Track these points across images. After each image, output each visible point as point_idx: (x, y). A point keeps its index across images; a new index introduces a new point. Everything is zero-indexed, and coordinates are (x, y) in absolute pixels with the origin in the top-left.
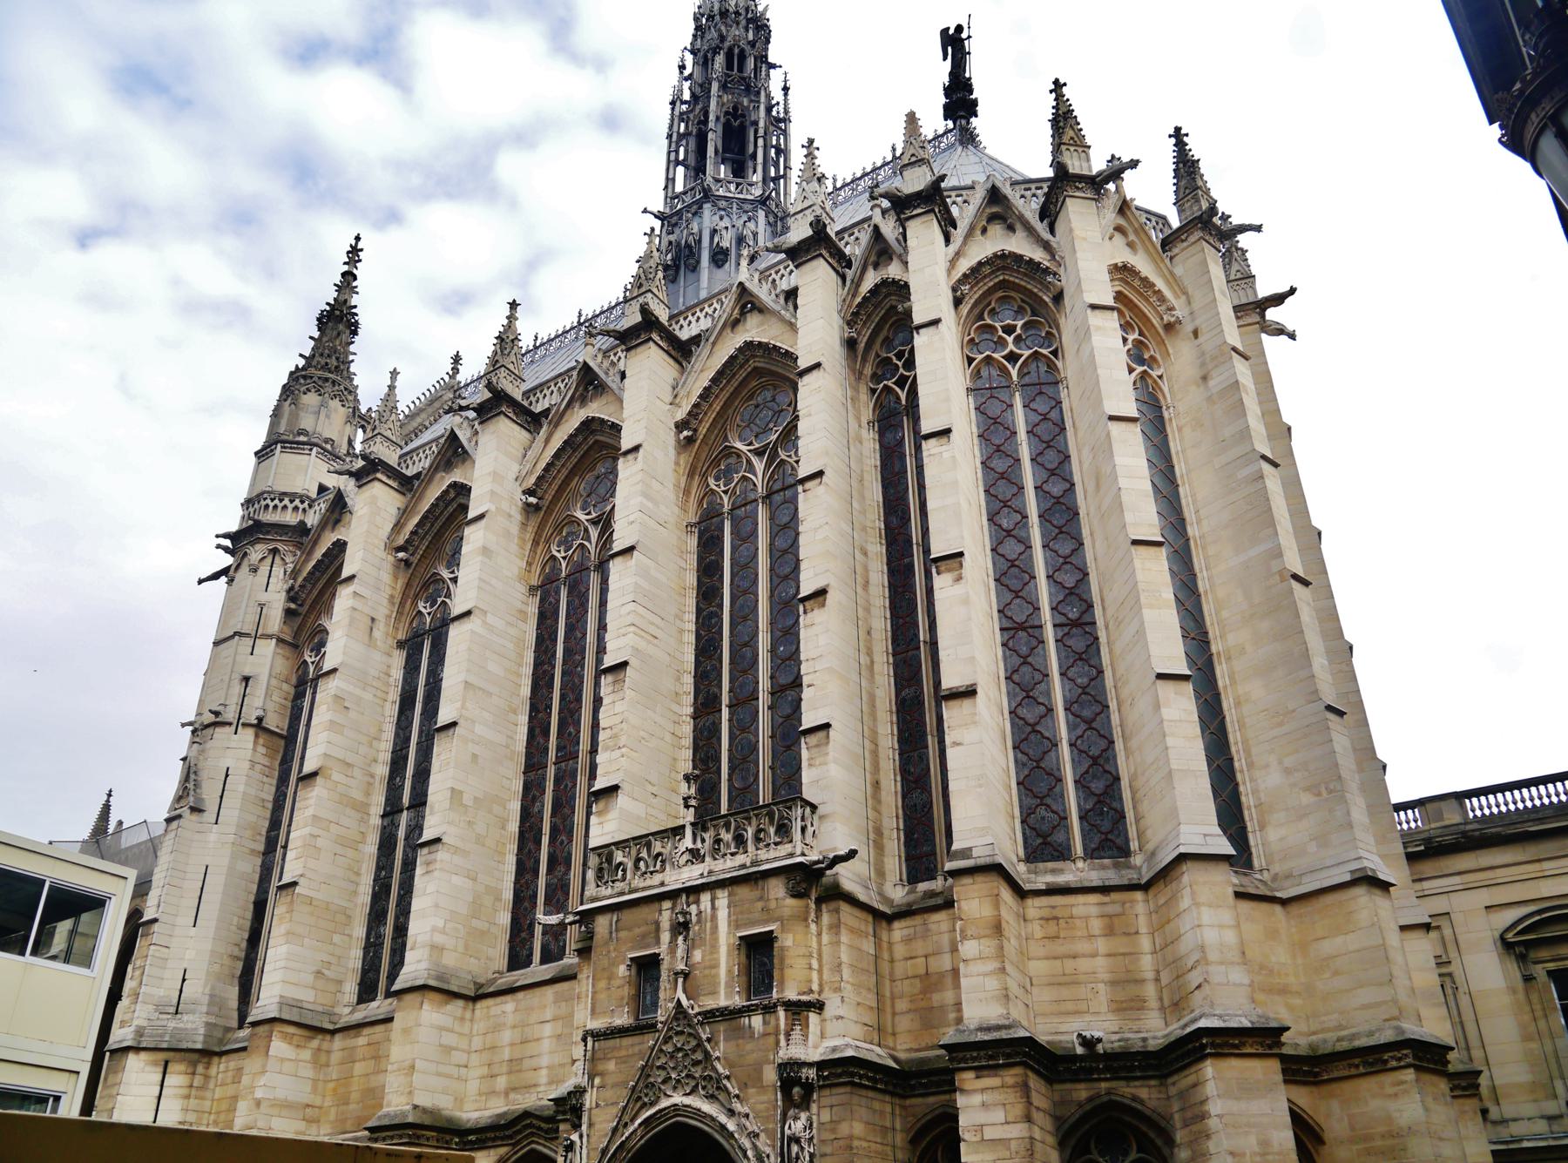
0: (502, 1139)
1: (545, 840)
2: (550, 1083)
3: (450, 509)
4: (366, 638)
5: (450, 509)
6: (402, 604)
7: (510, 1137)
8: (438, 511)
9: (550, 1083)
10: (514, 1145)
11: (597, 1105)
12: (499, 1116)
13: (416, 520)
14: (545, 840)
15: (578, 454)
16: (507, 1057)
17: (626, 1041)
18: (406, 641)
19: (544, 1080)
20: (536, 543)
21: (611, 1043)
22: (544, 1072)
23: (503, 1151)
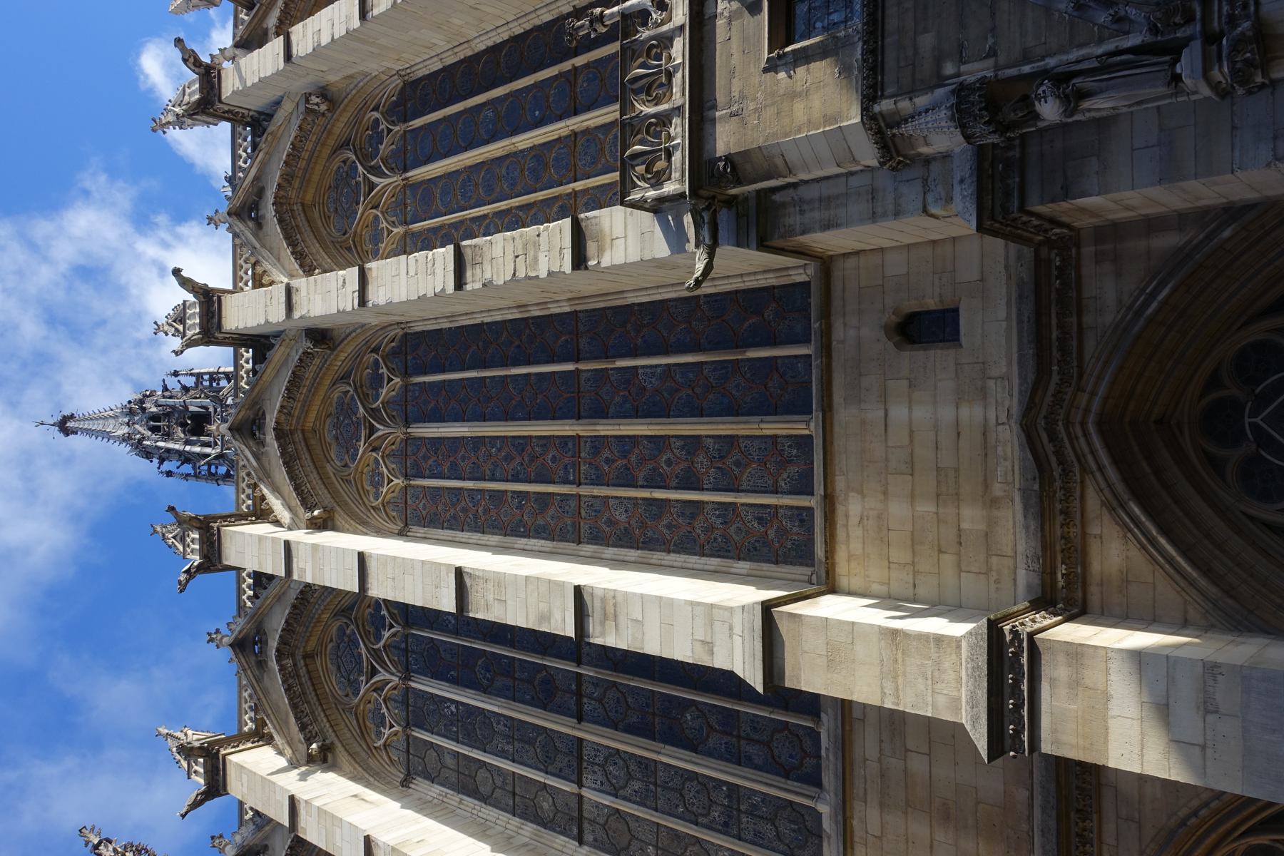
0: (1068, 493)
1: (659, 494)
2: (983, 394)
3: (303, 671)
4: (367, 805)
5: (303, 671)
6: (367, 769)
7: (1066, 473)
8: (297, 689)
9: (983, 394)
10: (1085, 470)
11: (992, 53)
12: (1026, 508)
13: (292, 720)
14: (659, 494)
15: (305, 455)
16: (931, 508)
17: (892, 23)
18: (409, 773)
19: (978, 411)
20: (363, 523)
21: (890, 56)
22: (965, 412)
23: (1093, 501)
